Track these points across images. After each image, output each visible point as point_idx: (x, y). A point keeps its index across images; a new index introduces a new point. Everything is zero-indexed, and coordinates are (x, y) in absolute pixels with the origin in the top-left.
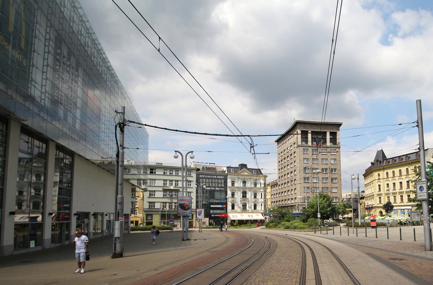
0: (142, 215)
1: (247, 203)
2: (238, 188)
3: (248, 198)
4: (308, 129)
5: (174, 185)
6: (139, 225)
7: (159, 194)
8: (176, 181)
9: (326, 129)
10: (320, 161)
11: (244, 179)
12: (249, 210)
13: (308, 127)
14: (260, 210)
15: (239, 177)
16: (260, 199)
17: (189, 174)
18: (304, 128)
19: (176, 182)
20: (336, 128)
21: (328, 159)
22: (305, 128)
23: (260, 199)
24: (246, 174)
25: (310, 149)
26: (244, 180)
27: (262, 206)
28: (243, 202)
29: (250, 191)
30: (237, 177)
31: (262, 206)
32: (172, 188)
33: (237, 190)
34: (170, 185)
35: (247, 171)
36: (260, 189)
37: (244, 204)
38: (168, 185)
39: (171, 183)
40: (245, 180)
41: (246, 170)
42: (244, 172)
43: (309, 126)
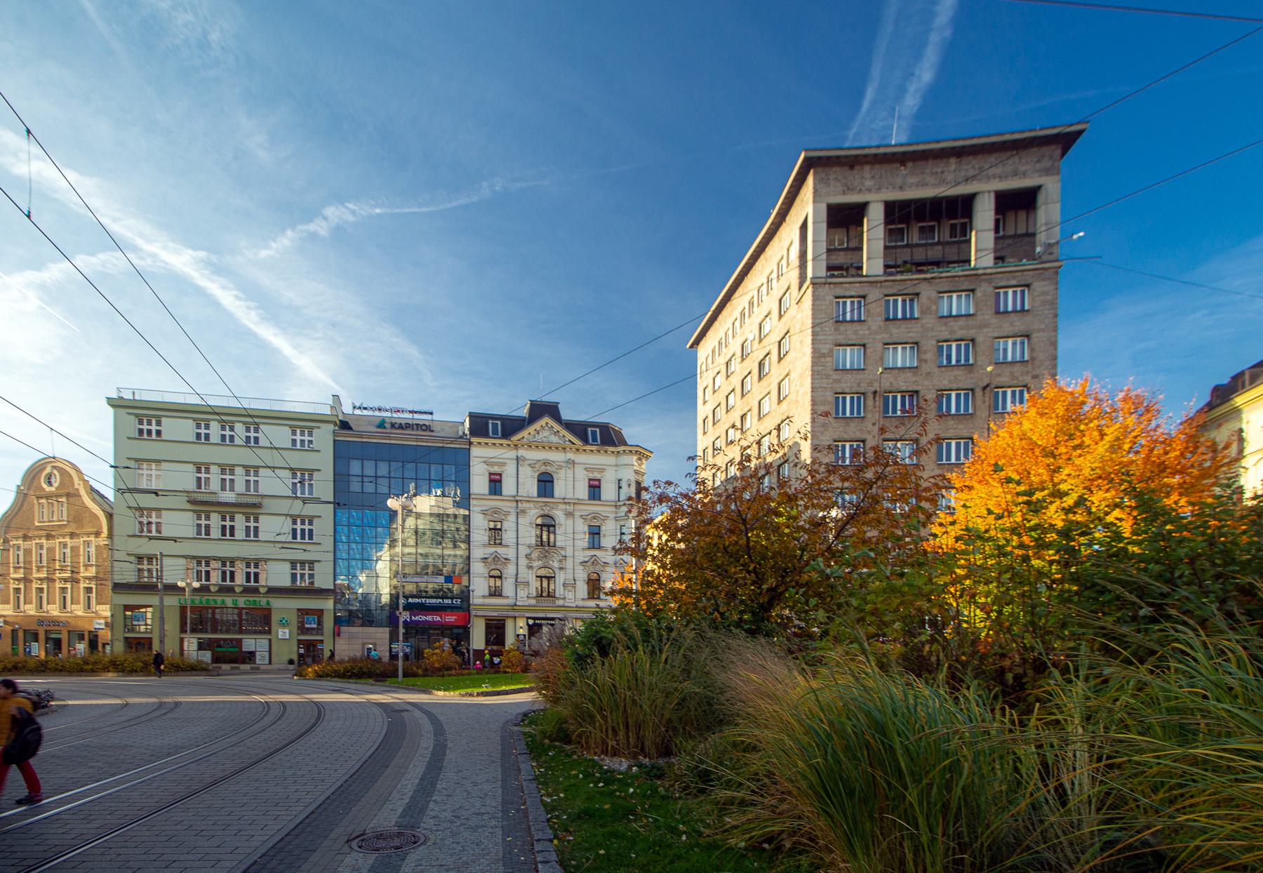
0: (108, 607)
4: (870, 190)
5: (240, 487)
6: (100, 648)
7: (179, 523)
8: (247, 468)
9: (974, 177)
10: (928, 356)
11: (546, 463)
13: (868, 183)
15: (522, 452)
17: (303, 441)
18: (844, 193)
19: (223, 472)
20: (1038, 166)
21: (980, 339)
22: (848, 189)
24: (554, 439)
25: (874, 294)
26: (543, 469)
30: (512, 454)
32: (228, 497)
34: (223, 489)
35: (557, 427)
38: (215, 485)
39: (228, 477)
40: (549, 469)
41: (552, 423)
42: (546, 433)
43: (873, 177)
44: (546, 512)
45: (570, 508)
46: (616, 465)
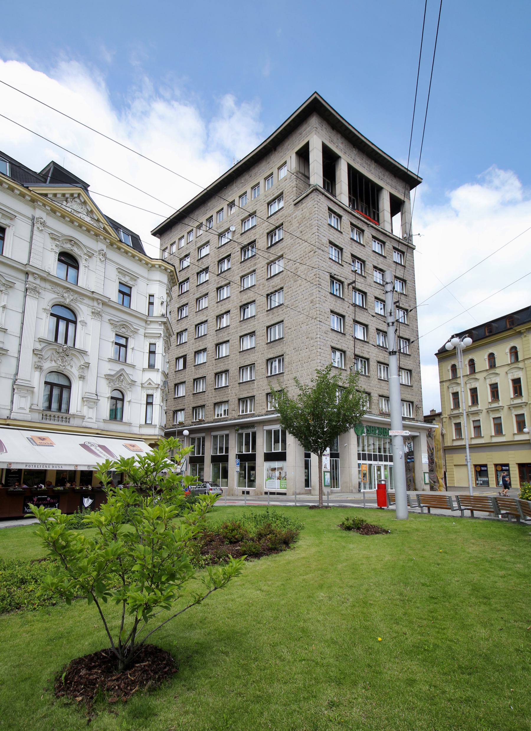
1: (74, 372)
2: (27, 274)
3: (83, 352)
11: (71, 241)
12: (83, 418)
14: (141, 426)
16: (144, 370)
23: (144, 370)
26: (68, 247)
27: (149, 404)
28: (48, 365)
29: (96, 314)
31: (149, 404)
33: (20, 286)
36: (147, 320)
37: (54, 379)
44: (67, 301)
45: (99, 307)
46: (148, 280)
